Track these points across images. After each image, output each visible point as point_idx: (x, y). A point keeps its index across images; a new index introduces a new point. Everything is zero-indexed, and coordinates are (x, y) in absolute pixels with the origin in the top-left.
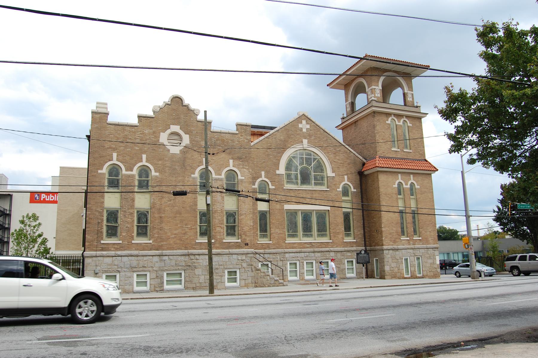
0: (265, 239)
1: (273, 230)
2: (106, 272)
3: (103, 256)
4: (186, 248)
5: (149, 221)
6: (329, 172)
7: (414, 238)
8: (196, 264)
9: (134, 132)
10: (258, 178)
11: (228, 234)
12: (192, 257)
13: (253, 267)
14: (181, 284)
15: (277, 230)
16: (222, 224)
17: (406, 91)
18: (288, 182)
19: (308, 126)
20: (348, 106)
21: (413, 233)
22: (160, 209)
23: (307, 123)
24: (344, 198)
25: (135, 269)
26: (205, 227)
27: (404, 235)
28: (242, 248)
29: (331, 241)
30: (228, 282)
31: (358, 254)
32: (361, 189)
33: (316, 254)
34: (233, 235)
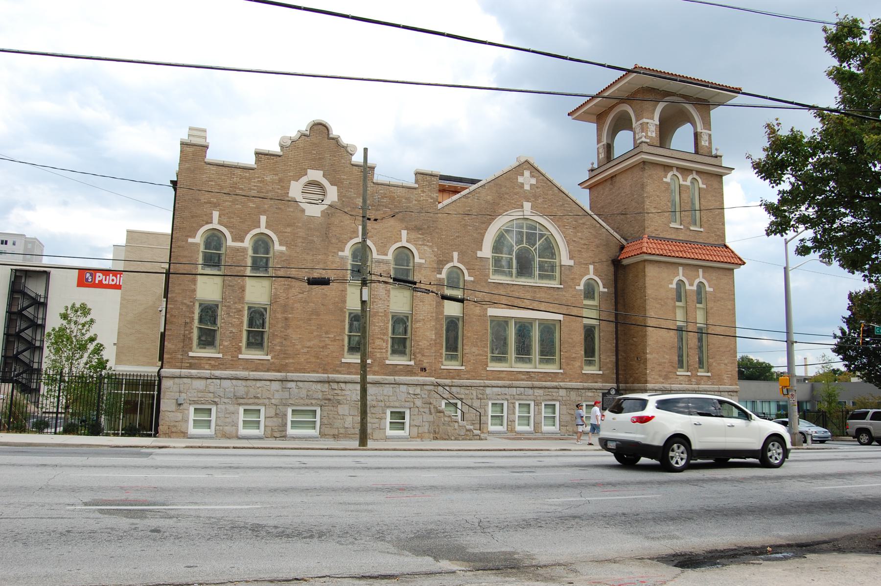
0: (453, 363)
1: (467, 349)
2: (195, 402)
3: (191, 377)
4: (325, 371)
5: (267, 325)
6: (565, 258)
7: (699, 374)
8: (339, 398)
9: (249, 179)
10: (448, 262)
11: (394, 352)
12: (335, 386)
13: (432, 407)
14: (314, 428)
15: (474, 349)
16: (384, 334)
17: (699, 130)
18: (496, 272)
19: (533, 181)
20: (601, 150)
21: (697, 366)
22: (285, 306)
23: (532, 176)
24: (586, 302)
25: (241, 401)
26: (357, 338)
27: (682, 367)
28: (415, 374)
29: (561, 371)
30: (391, 429)
31: (604, 395)
32: (616, 288)
33: (536, 391)
34: (402, 353)
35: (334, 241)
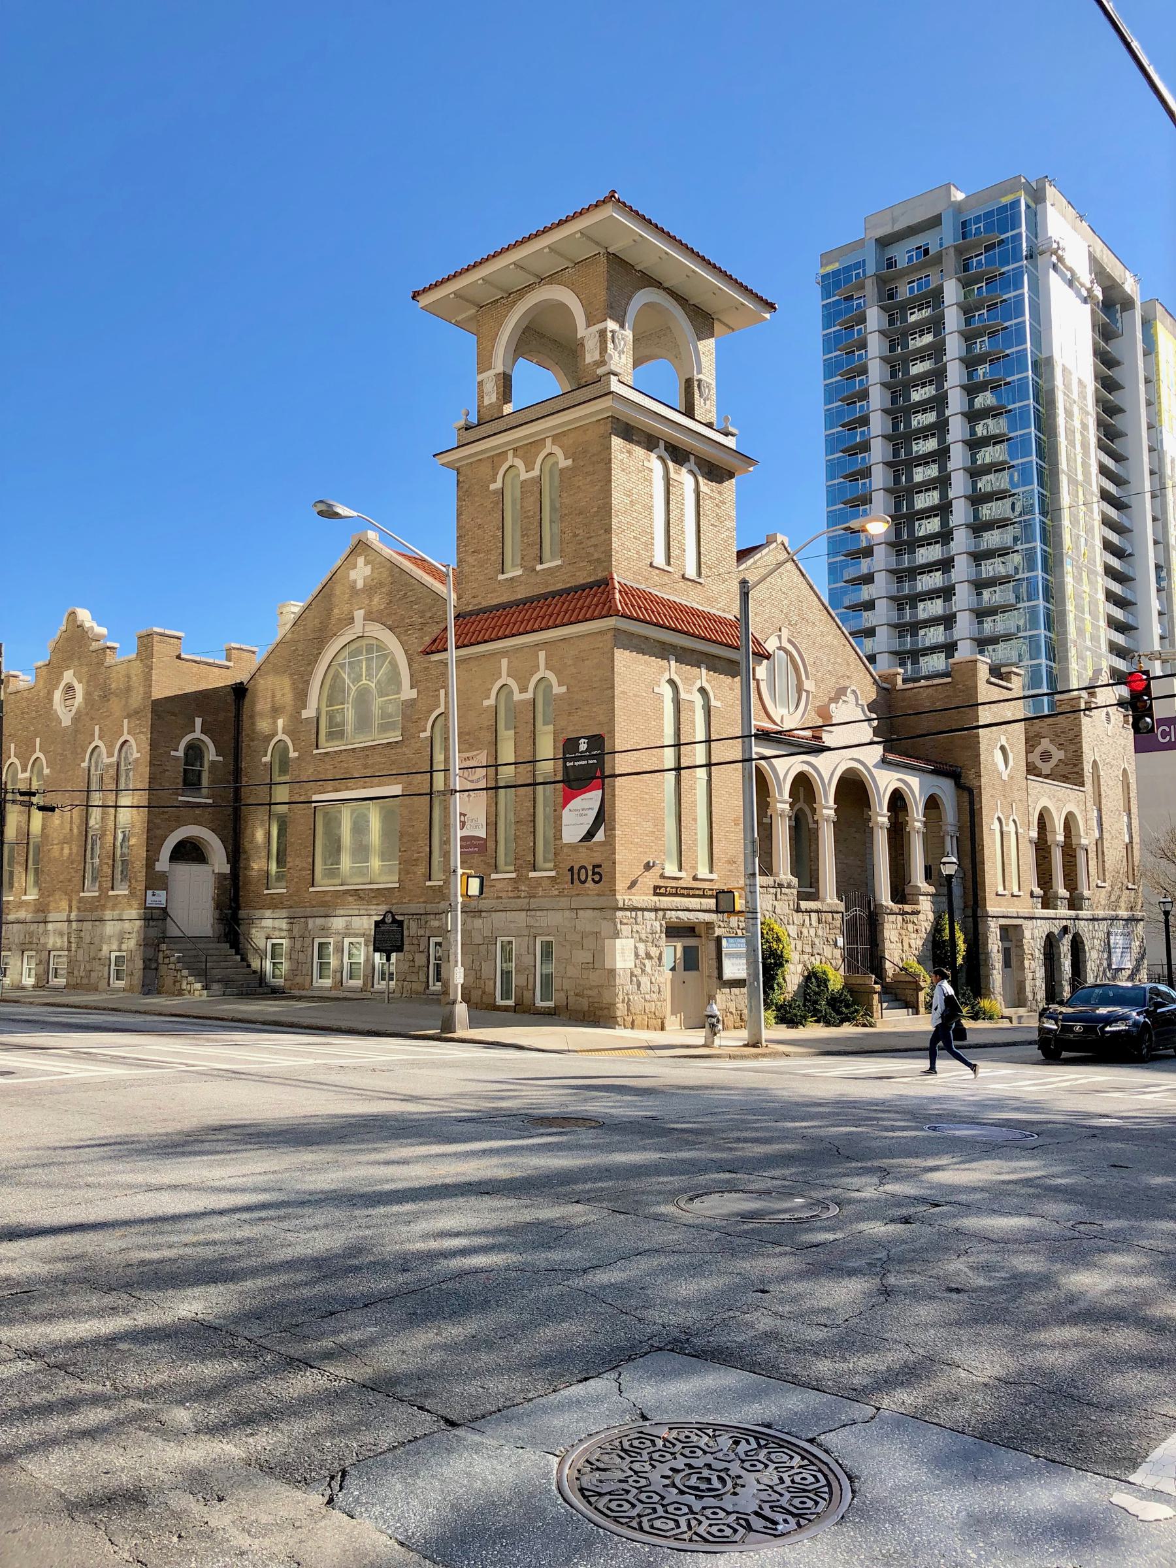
35: (79, 750)
